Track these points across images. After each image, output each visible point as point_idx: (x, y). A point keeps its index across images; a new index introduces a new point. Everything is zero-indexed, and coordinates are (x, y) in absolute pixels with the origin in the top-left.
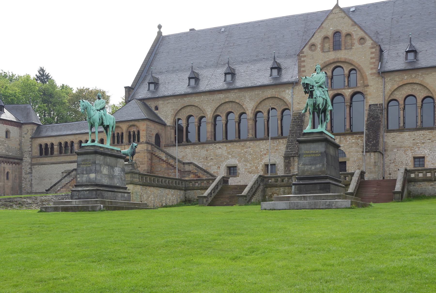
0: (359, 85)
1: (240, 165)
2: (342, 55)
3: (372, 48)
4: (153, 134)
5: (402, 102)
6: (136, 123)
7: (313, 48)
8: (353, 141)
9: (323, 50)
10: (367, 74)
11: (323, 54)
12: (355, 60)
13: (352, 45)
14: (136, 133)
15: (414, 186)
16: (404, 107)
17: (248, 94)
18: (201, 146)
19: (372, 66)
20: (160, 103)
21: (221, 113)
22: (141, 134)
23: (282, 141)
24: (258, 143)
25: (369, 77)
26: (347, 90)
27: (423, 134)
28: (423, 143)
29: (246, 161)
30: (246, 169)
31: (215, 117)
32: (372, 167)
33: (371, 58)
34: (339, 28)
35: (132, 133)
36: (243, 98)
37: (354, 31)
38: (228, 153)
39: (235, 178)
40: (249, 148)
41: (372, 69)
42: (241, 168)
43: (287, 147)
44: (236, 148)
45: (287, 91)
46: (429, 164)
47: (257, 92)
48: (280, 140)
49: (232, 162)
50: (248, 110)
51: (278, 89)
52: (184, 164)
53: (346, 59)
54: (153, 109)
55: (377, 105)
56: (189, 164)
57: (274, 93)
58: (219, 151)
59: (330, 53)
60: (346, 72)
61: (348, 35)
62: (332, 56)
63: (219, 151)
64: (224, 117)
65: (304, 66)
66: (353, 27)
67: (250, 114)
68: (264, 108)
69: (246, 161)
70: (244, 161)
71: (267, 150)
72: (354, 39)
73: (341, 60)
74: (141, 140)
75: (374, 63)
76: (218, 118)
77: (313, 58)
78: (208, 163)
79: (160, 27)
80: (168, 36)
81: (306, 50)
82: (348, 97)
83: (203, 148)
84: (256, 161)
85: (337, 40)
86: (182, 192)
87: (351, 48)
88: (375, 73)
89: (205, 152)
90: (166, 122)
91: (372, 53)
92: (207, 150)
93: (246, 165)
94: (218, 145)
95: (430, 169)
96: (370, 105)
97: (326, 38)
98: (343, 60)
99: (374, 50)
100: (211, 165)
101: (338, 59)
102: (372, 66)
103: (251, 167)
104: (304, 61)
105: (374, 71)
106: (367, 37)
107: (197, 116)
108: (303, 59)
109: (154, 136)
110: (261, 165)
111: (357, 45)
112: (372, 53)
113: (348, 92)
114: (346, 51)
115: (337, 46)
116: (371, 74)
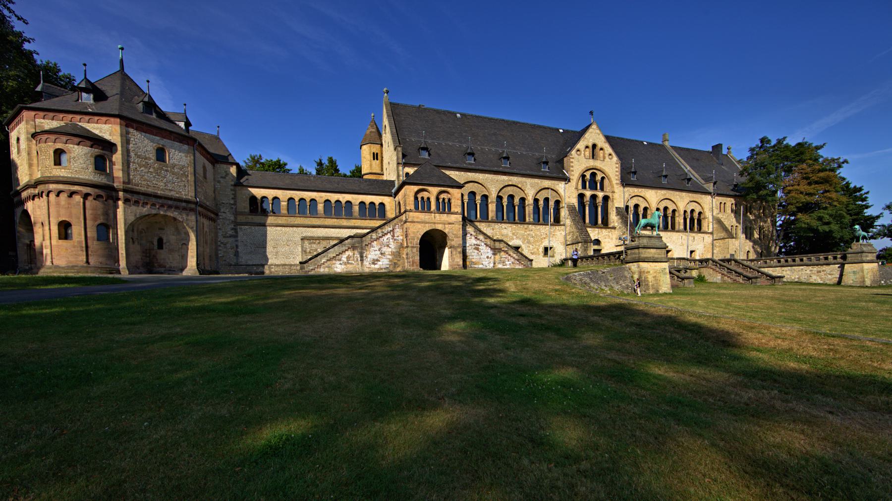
1: (523, 246)
2: (598, 164)
6: (449, 189)
13: (604, 158)
14: (446, 201)
17: (529, 181)
24: (538, 227)
25: (615, 186)
29: (529, 242)
34: (596, 142)
44: (520, 229)
47: (536, 180)
51: (553, 182)
52: (495, 241)
56: (500, 241)
61: (601, 149)
62: (592, 163)
63: (505, 232)
69: (529, 242)
81: (573, 152)
83: (489, 226)
94: (504, 225)
97: (587, 147)
106: (613, 154)
111: (607, 159)
113: (600, 195)
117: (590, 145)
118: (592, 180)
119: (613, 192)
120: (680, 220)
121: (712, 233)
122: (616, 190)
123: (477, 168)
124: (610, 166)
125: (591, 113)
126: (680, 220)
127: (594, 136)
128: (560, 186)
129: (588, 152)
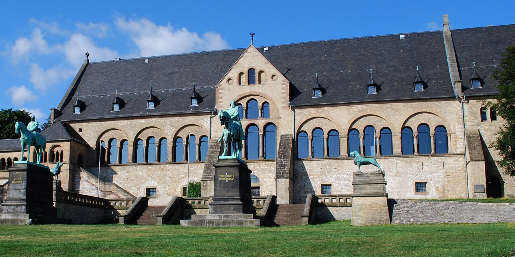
0: (271, 117)
3: (283, 84)
4: (76, 155)
5: (310, 134)
7: (230, 81)
8: (266, 168)
9: (240, 84)
10: (279, 107)
11: (239, 87)
12: (269, 94)
13: (266, 80)
15: (321, 211)
16: (312, 138)
18: (122, 167)
19: (283, 100)
20: (84, 125)
21: (143, 137)
22: (64, 155)
23: (199, 166)
24: (177, 166)
25: (281, 110)
26: (261, 121)
27: (330, 164)
28: (330, 172)
29: (165, 183)
30: (165, 191)
31: (137, 141)
32: (283, 193)
33: (282, 93)
35: (55, 153)
36: (164, 124)
37: (267, 68)
38: (149, 175)
39: (154, 200)
40: (169, 171)
41: (283, 103)
42: (160, 190)
43: (205, 171)
44: (156, 170)
45: (205, 120)
46: (334, 191)
47: (177, 119)
48: (198, 164)
49: (151, 184)
50: (168, 135)
51: (197, 117)
53: (259, 93)
54: (77, 131)
55: (287, 135)
57: (193, 120)
58: (140, 173)
59: (245, 87)
60: (260, 105)
64: (145, 142)
65: (221, 98)
66: (265, 65)
67: (170, 140)
68: (183, 134)
70: (164, 183)
71: (186, 173)
72: (267, 76)
73: (255, 94)
74: (64, 160)
75: (285, 97)
76: (139, 142)
77: (230, 91)
78: (129, 184)
79: (88, 55)
80: (95, 63)
81: (224, 82)
82: (261, 128)
83: (124, 169)
84: (175, 184)
85: (252, 76)
86: (103, 211)
87: (264, 84)
88: (285, 107)
89: (126, 174)
90: (89, 143)
91: (283, 89)
92: (128, 172)
93: (166, 187)
95: (336, 196)
96: (282, 136)
98: (257, 94)
99: (285, 86)
100: (131, 187)
101: (252, 92)
102: (283, 100)
103: (170, 189)
104: (221, 93)
105: (285, 105)
107: (119, 139)
108: (220, 91)
109: (77, 156)
110: (179, 188)
112: (283, 89)
113: (261, 123)
114: (260, 86)
115: (251, 81)
116: (282, 107)
117: (246, 71)
118: (251, 106)
119: (279, 118)
120: (397, 142)
121: (462, 155)
122: (282, 115)
123: (124, 115)
124: (274, 88)
125: (253, 35)
126: (397, 142)
127: (252, 59)
128: (204, 121)
129: (244, 79)
